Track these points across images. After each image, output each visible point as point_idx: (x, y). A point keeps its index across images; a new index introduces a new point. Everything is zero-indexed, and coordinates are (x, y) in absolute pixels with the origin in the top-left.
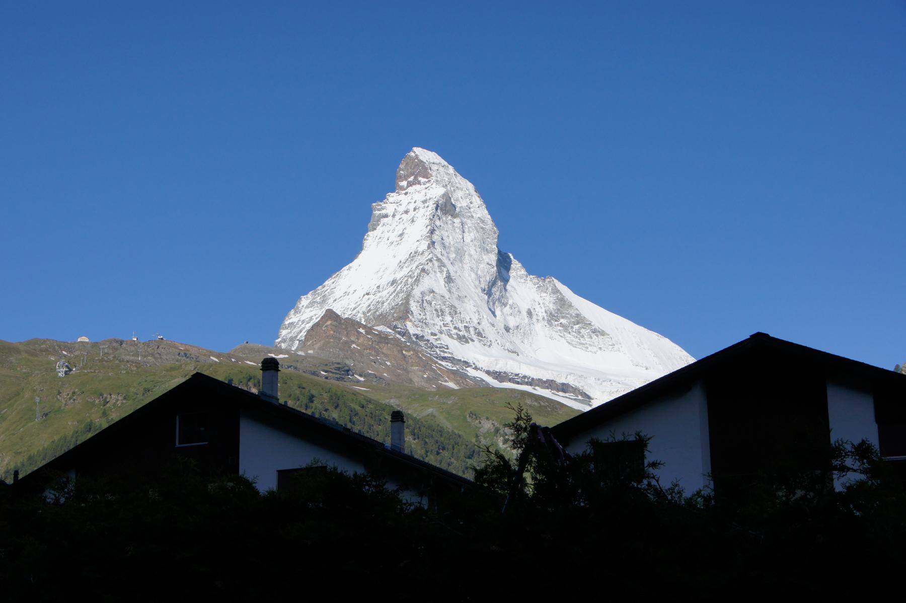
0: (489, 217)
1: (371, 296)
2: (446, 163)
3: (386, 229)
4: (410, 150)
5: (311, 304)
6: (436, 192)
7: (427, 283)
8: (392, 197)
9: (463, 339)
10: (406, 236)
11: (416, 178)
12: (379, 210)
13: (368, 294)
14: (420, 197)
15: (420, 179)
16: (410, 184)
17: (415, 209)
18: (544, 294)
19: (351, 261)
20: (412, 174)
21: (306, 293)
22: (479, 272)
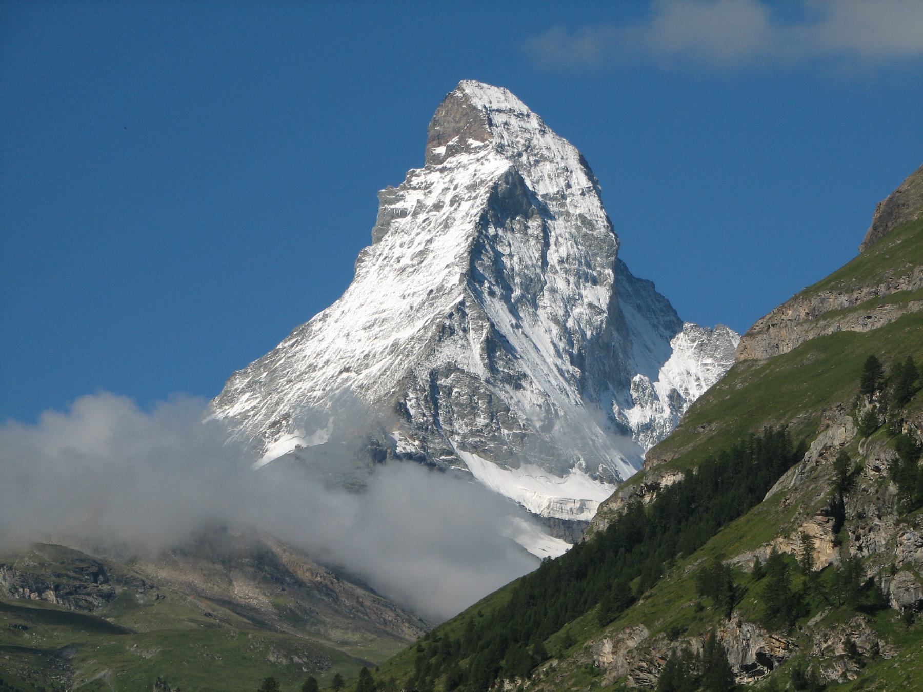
0: (602, 213)
1: (353, 374)
2: (524, 109)
3: (398, 239)
4: (456, 86)
5: (250, 387)
6: (496, 166)
7: (448, 352)
8: (420, 177)
9: (506, 460)
10: (431, 256)
11: (462, 140)
13: (347, 370)
14: (463, 178)
15: (470, 141)
17: (452, 203)
18: (709, 361)
19: (329, 303)
20: (457, 132)
21: (244, 364)
22: (570, 324)
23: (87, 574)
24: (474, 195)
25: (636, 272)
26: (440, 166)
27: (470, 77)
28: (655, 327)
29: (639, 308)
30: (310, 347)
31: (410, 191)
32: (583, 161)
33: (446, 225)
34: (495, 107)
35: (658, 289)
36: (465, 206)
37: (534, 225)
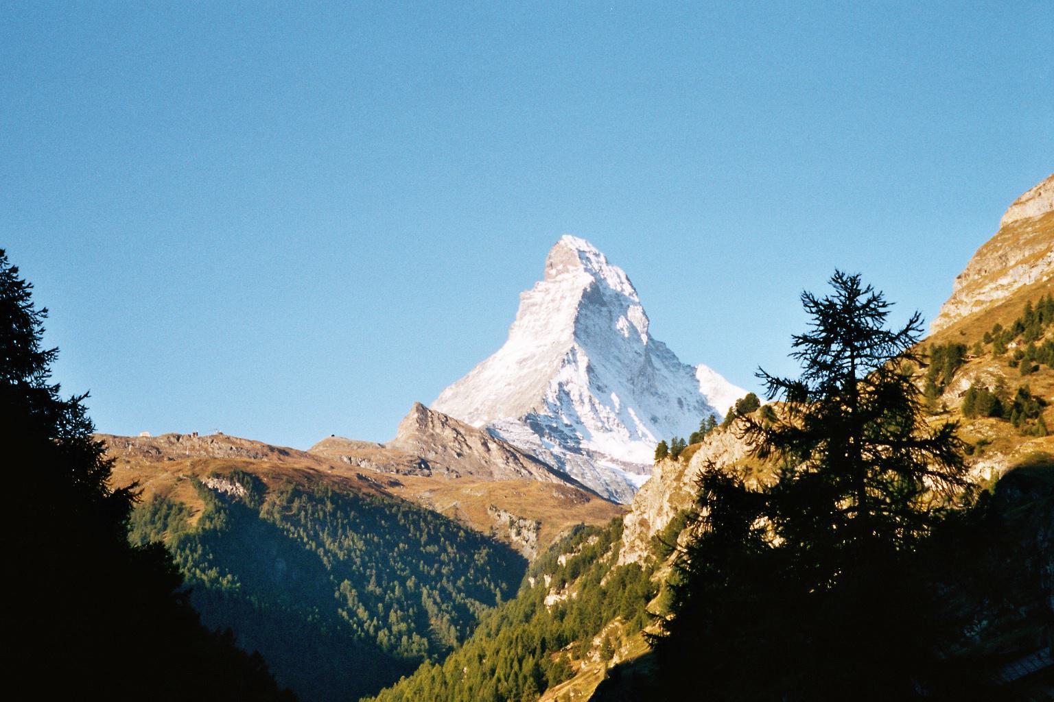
1: (512, 387)
4: (560, 238)
8: (542, 285)
12: (527, 299)
13: (509, 384)
15: (569, 267)
16: (559, 273)
19: (496, 350)
23: (416, 464)
24: (573, 294)
25: (656, 338)
26: (553, 280)
27: (568, 233)
28: (667, 367)
29: (658, 356)
30: (487, 374)
31: (538, 293)
32: (628, 279)
33: (558, 310)
34: (582, 249)
35: (667, 347)
36: (568, 300)
37: (604, 309)
